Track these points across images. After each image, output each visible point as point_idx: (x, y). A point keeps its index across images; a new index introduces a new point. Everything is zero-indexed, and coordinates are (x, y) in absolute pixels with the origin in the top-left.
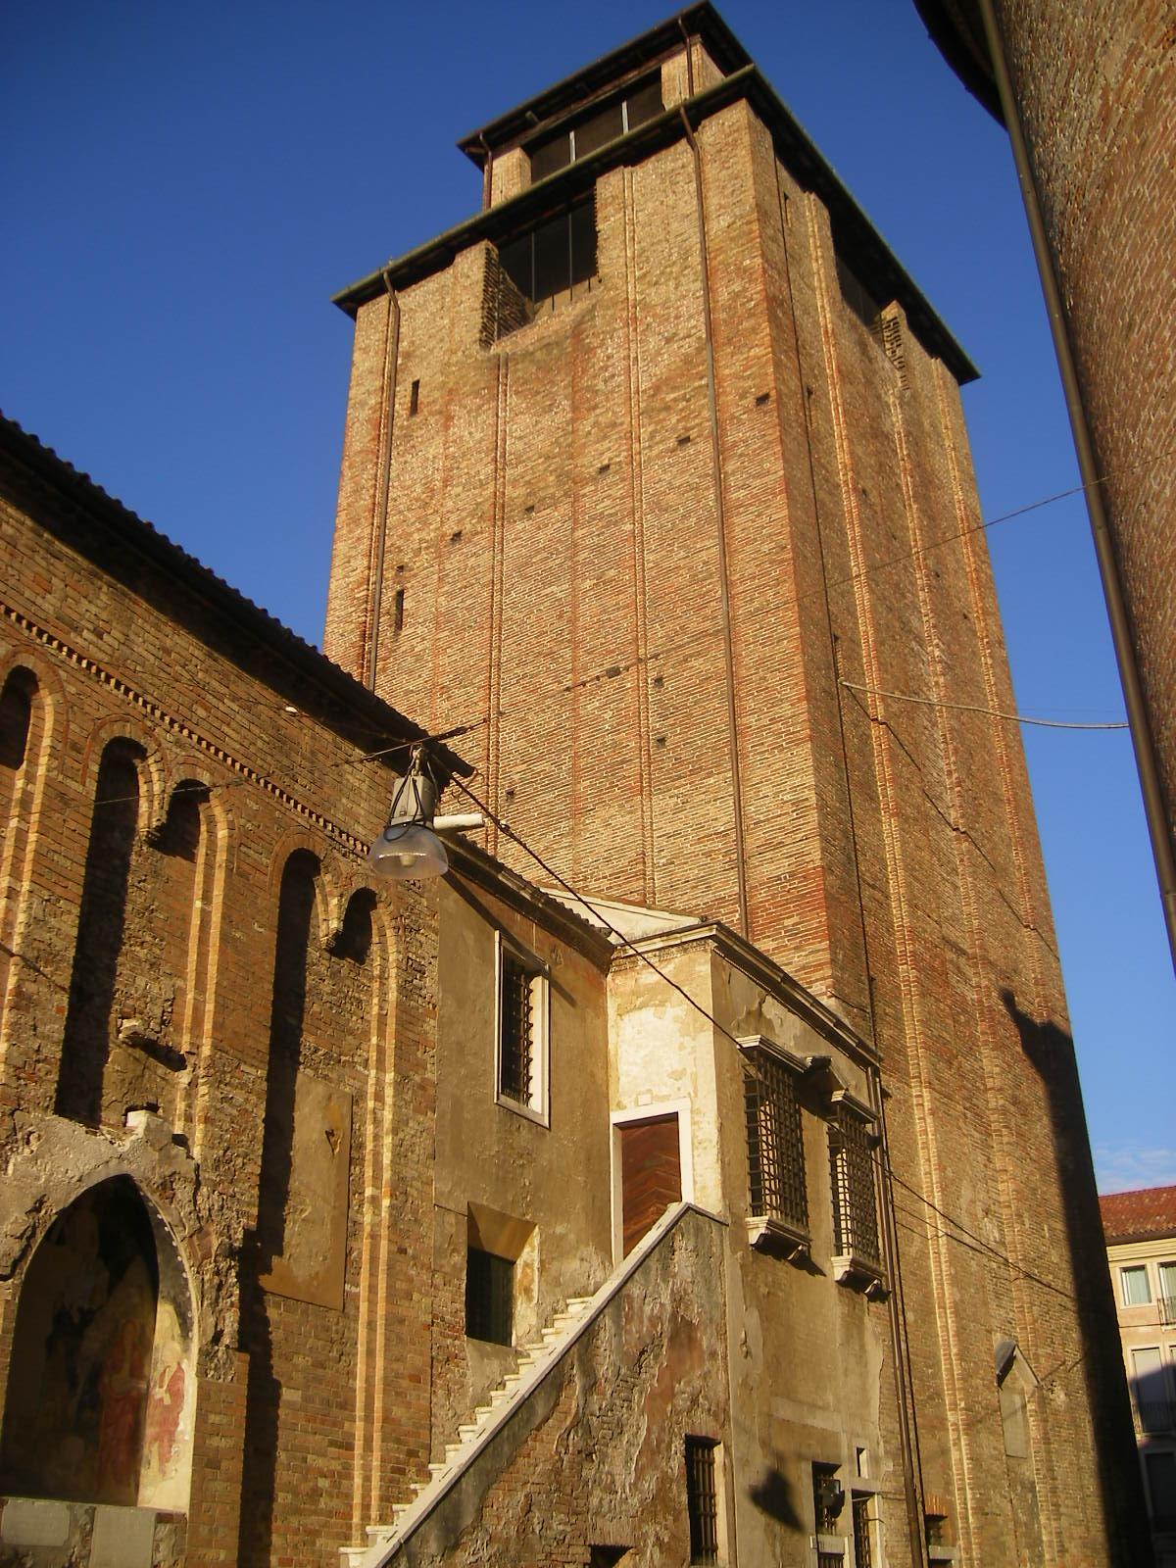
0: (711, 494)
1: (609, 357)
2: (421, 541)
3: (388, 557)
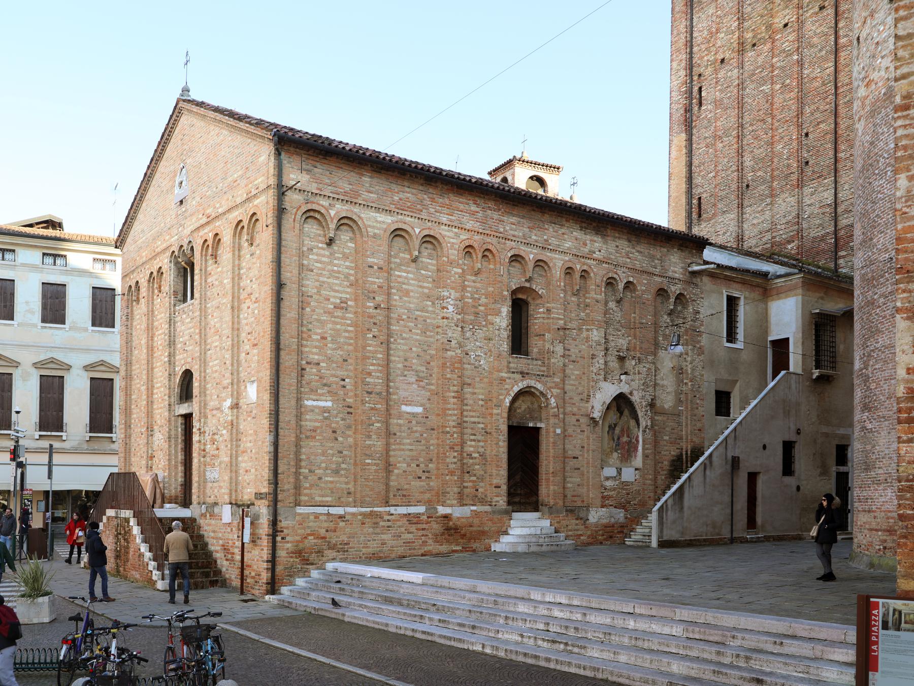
0: (832, 38)
2: (708, 61)
3: (694, 69)
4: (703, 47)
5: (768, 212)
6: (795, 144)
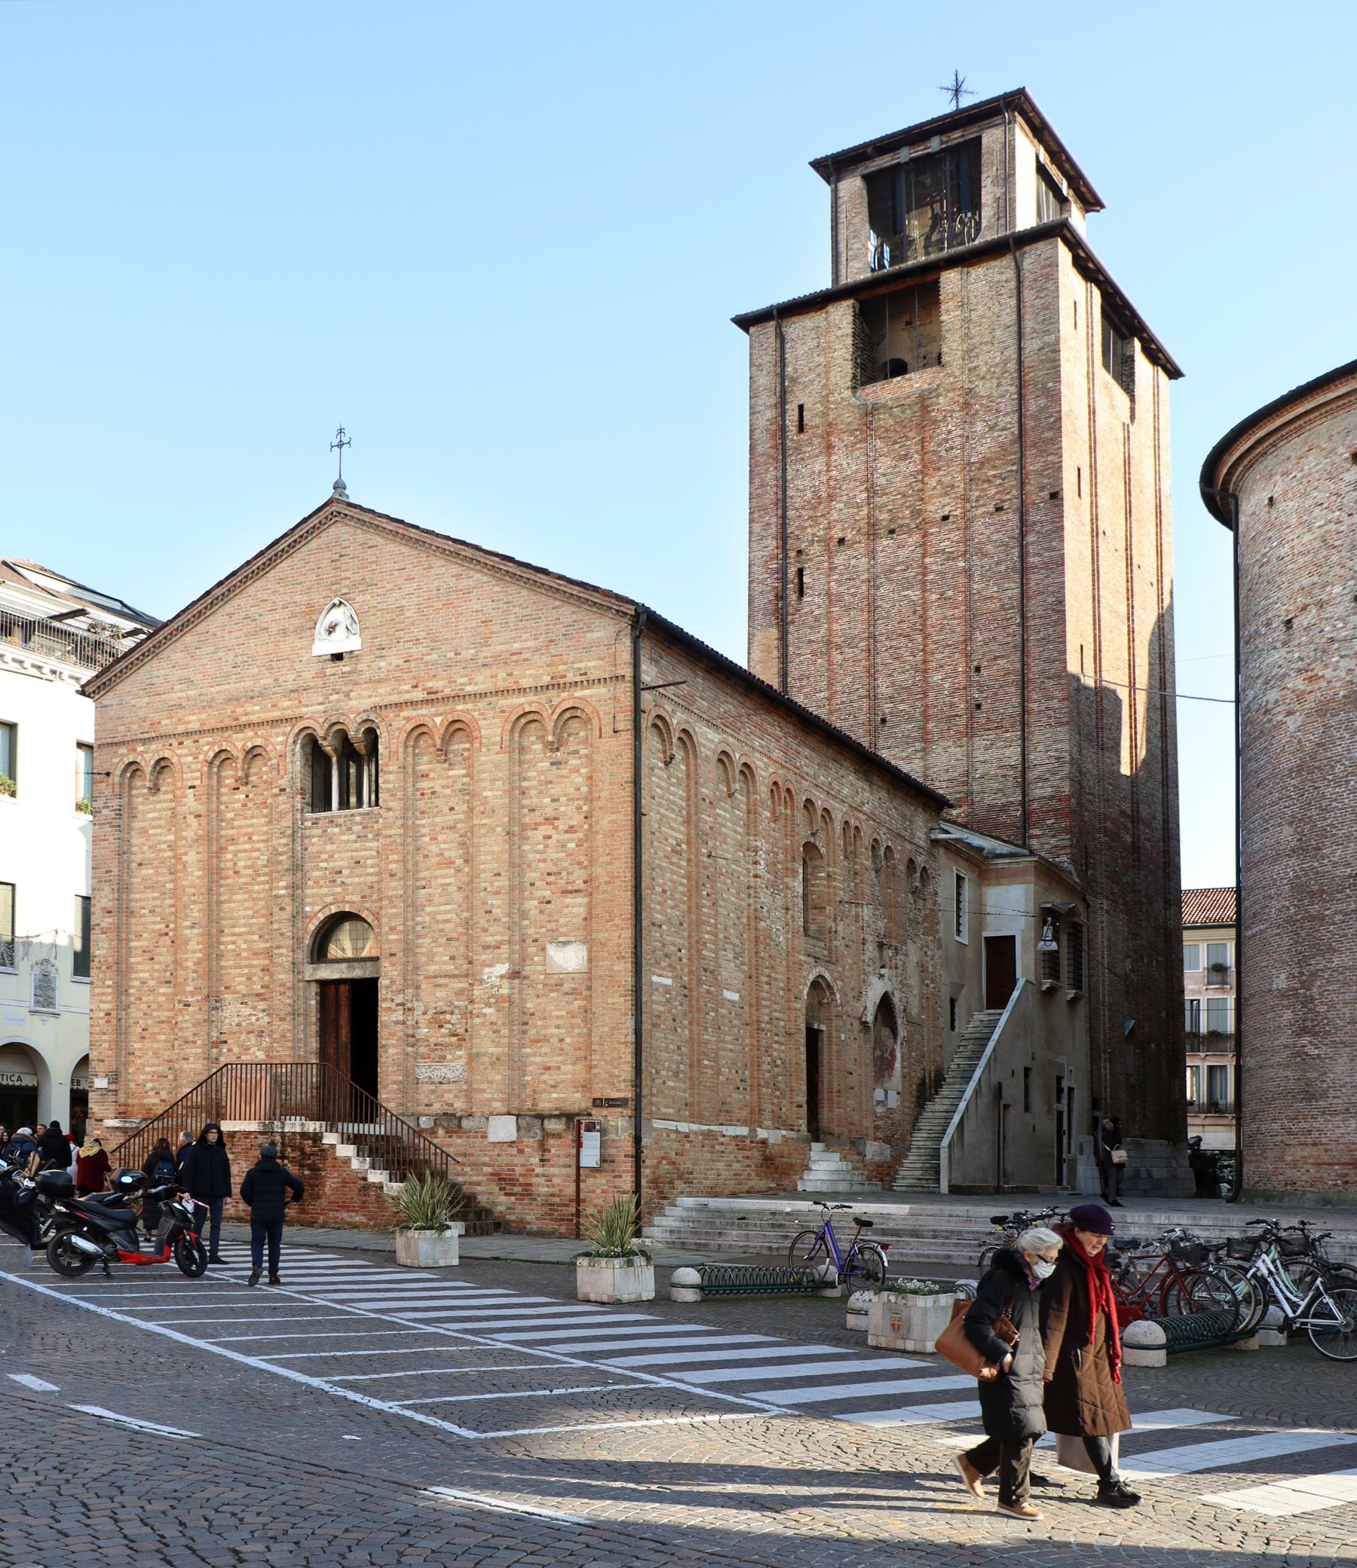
0: (1016, 552)
1: (950, 432)
2: (814, 535)
3: (790, 541)
4: (805, 514)
5: (917, 761)
6: (961, 678)
